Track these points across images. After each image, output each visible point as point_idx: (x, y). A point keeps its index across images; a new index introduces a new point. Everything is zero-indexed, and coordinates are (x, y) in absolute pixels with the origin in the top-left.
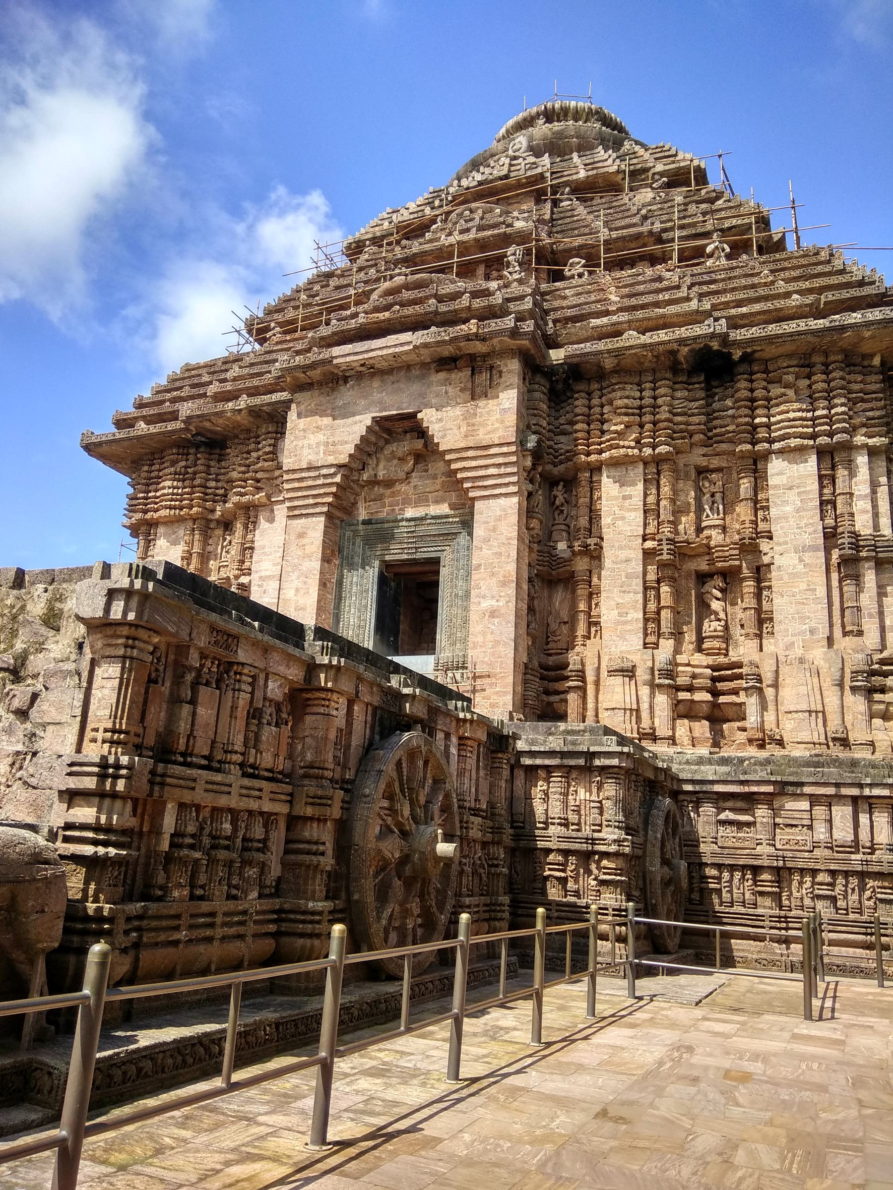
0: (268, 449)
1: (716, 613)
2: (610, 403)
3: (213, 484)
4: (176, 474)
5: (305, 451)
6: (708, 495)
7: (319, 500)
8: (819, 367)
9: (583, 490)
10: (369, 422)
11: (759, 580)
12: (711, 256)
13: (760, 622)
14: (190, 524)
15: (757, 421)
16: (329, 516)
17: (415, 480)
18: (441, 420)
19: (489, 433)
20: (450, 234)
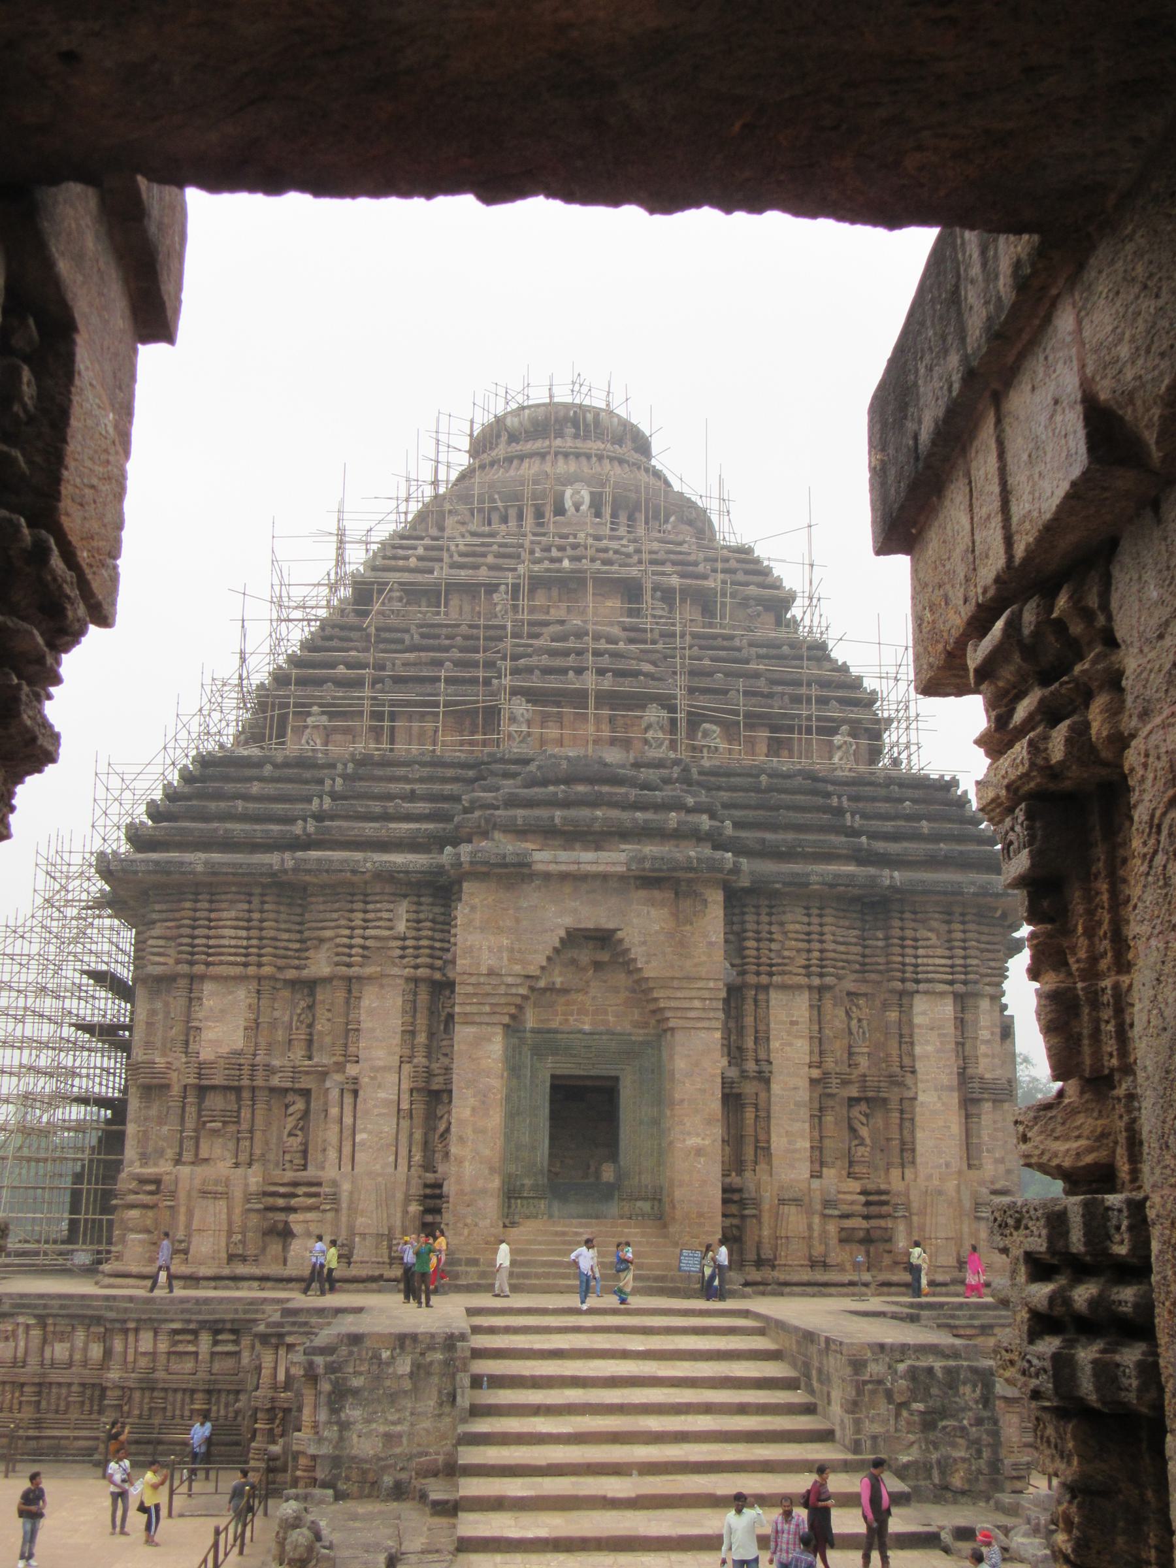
0: (385, 915)
1: (863, 1139)
2: (782, 924)
3: (286, 936)
4: (237, 919)
5: (485, 955)
6: (854, 1022)
7: (498, 1010)
8: (957, 917)
9: (749, 1007)
10: (563, 933)
11: (902, 1112)
12: (839, 748)
13: (902, 1150)
14: (253, 986)
15: (908, 960)
16: (506, 1026)
17: (593, 992)
18: (644, 943)
19: (696, 965)
20: (580, 671)
